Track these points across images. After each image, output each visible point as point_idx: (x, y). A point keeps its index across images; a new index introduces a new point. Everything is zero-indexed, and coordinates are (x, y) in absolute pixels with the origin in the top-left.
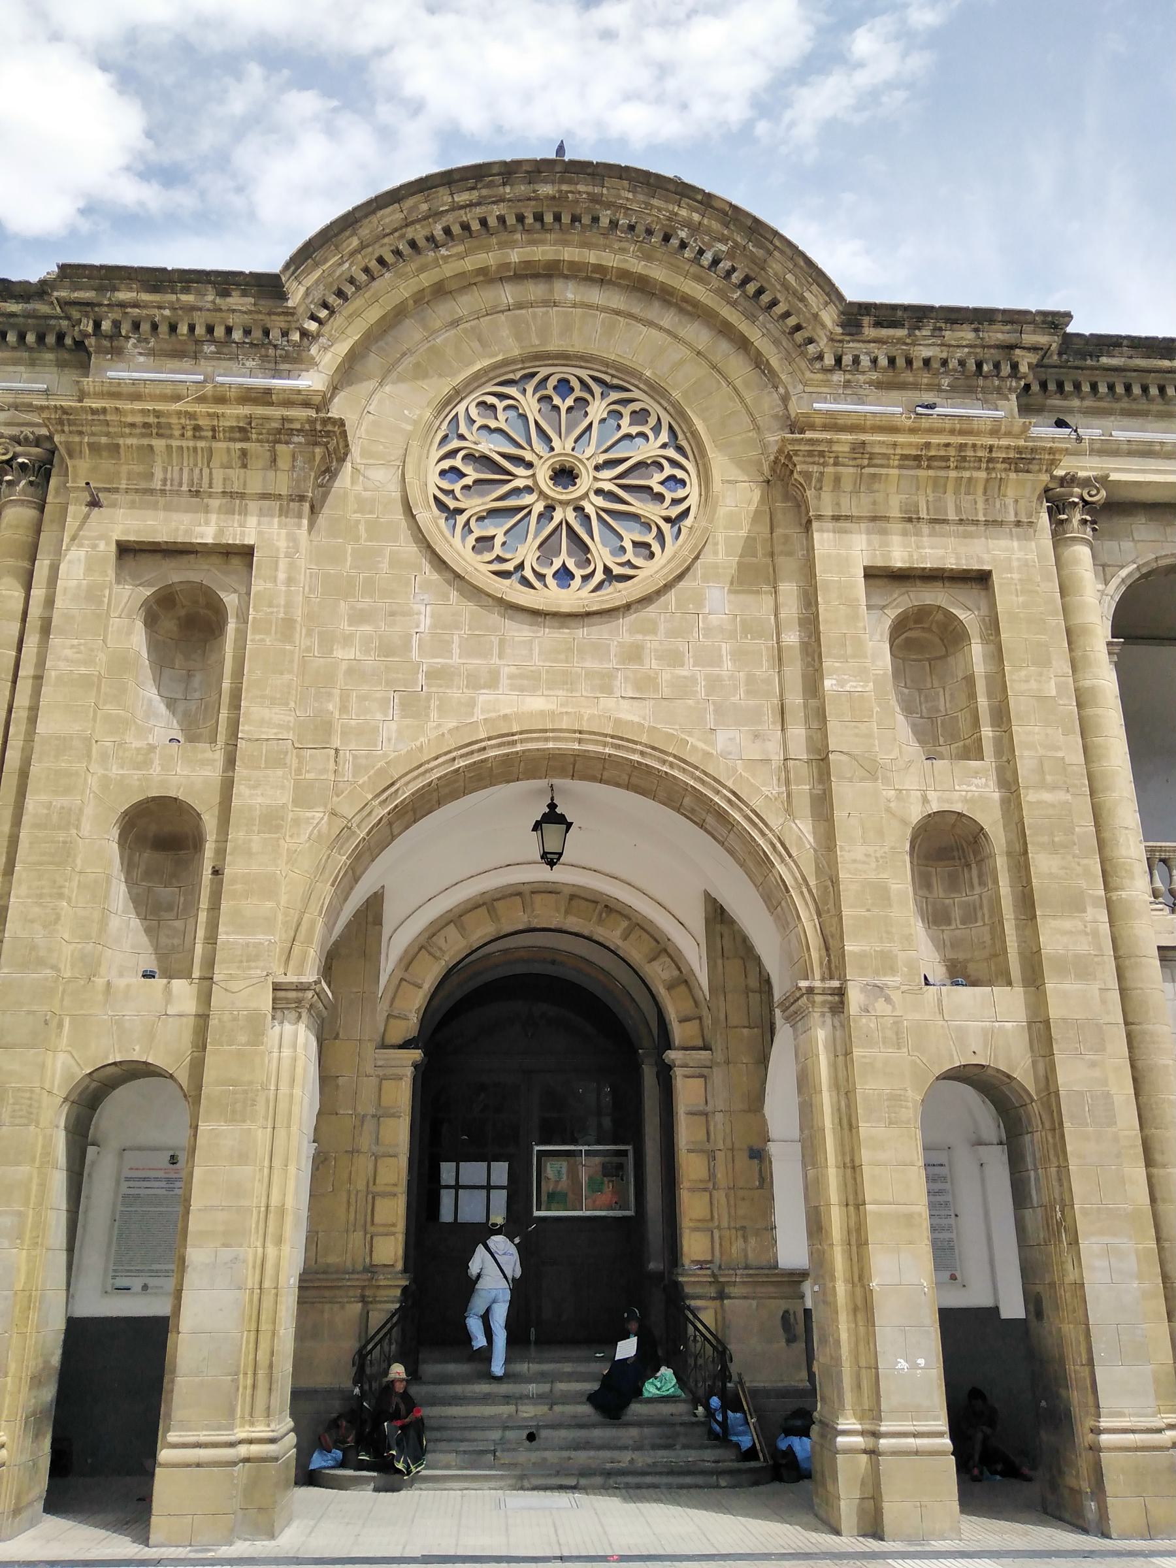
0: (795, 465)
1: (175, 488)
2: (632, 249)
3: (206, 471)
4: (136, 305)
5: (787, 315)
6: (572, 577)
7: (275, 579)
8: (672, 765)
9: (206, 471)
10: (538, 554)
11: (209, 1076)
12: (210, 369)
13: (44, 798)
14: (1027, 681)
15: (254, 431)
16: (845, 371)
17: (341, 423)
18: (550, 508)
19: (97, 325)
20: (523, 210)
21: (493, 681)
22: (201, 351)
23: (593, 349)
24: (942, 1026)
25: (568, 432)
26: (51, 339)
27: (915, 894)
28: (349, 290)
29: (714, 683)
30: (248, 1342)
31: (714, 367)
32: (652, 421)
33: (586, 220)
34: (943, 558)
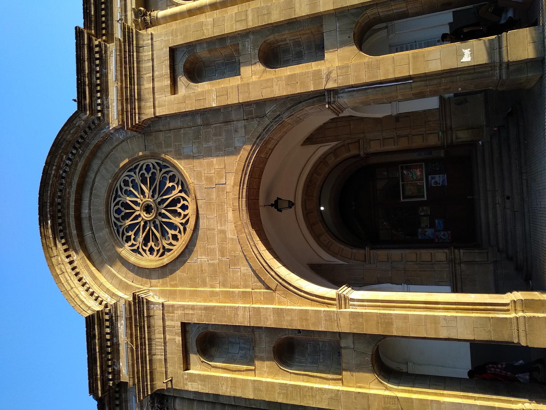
0: (137, 124)
1: (163, 351)
2: (68, 190)
3: (157, 340)
4: (101, 367)
6: (184, 204)
7: (191, 314)
8: (249, 163)
9: (157, 340)
11: (375, 332)
12: (122, 340)
13: (276, 395)
14: (208, 30)
15: (140, 324)
19: (110, 380)
20: (58, 230)
25: (133, 209)
27: (291, 65)
28: (91, 290)
31: (107, 157)
32: (127, 178)
33: (59, 207)
34: (166, 67)
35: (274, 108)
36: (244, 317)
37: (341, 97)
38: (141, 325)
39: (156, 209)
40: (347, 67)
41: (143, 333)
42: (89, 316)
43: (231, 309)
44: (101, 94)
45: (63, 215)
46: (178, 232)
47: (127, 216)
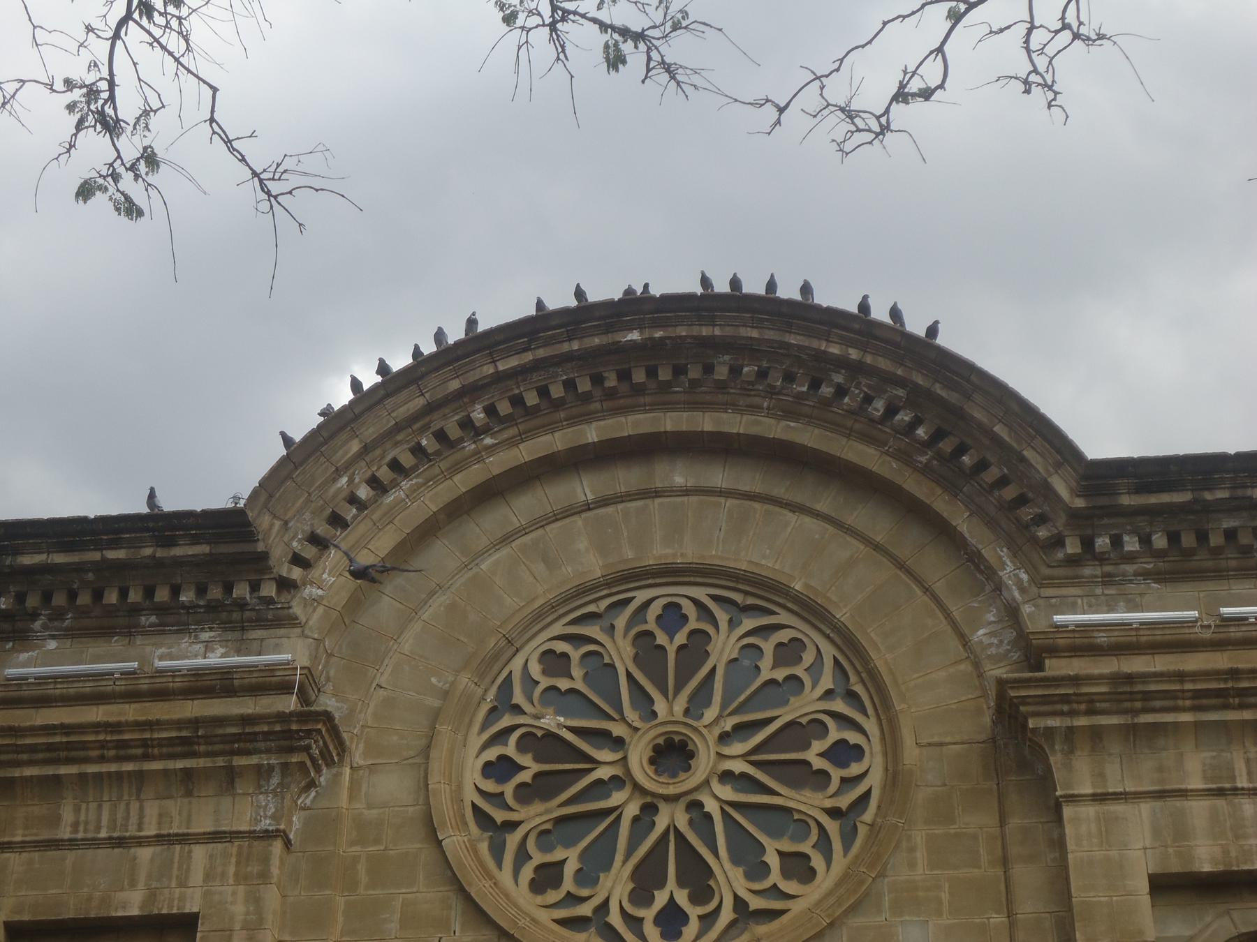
1: (90, 835)
3: (135, 806)
5: (1003, 482)
6: (685, 918)
9: (135, 806)
10: (631, 886)
12: (148, 649)
15: (201, 741)
16: (1101, 559)
17: (327, 717)
18: (650, 809)
20: (601, 369)
22: (137, 625)
23: (717, 553)
25: (678, 690)
28: (350, 513)
31: (901, 566)
38: (199, 744)
39: (672, 790)
41: (165, 750)
42: (249, 524)
44: (1159, 554)
45: (665, 387)
46: (568, 892)
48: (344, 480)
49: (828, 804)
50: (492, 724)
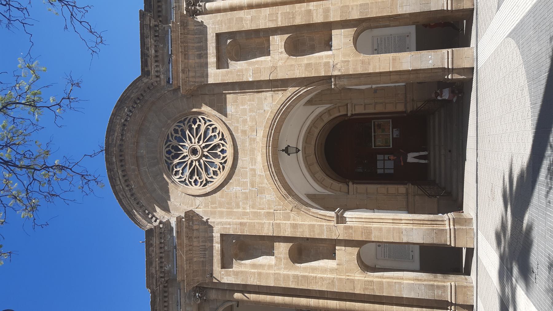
3: (201, 247)
6: (223, 149)
7: (229, 228)
8: (275, 122)
9: (201, 247)
10: (217, 158)
11: (360, 239)
12: (171, 248)
13: (290, 283)
14: (247, 24)
15: (189, 235)
19: (162, 277)
21: (254, 170)
24: (343, 49)
26: (166, 289)
29: (251, 110)
30: (426, 226)
35: (295, 84)
36: (268, 230)
37: (343, 81)
40: (348, 61)
43: (259, 224)
47: (177, 156)
48: (140, 213)
49: (203, 124)
50: (188, 184)
